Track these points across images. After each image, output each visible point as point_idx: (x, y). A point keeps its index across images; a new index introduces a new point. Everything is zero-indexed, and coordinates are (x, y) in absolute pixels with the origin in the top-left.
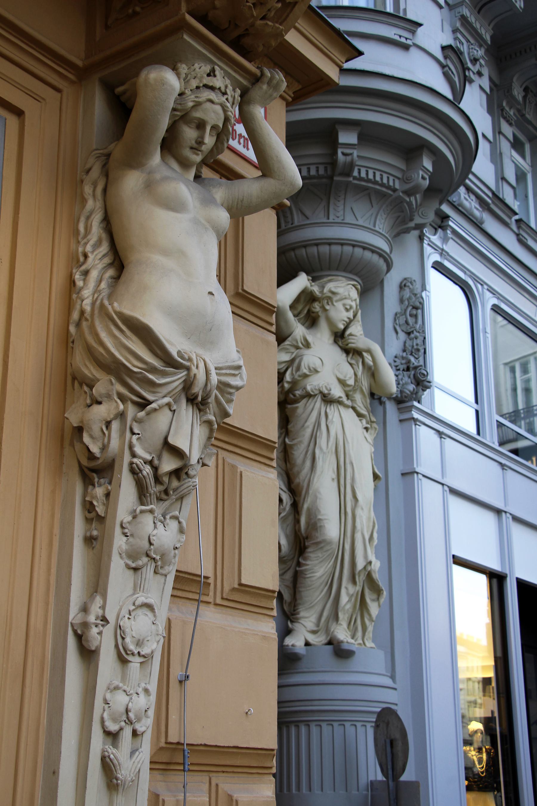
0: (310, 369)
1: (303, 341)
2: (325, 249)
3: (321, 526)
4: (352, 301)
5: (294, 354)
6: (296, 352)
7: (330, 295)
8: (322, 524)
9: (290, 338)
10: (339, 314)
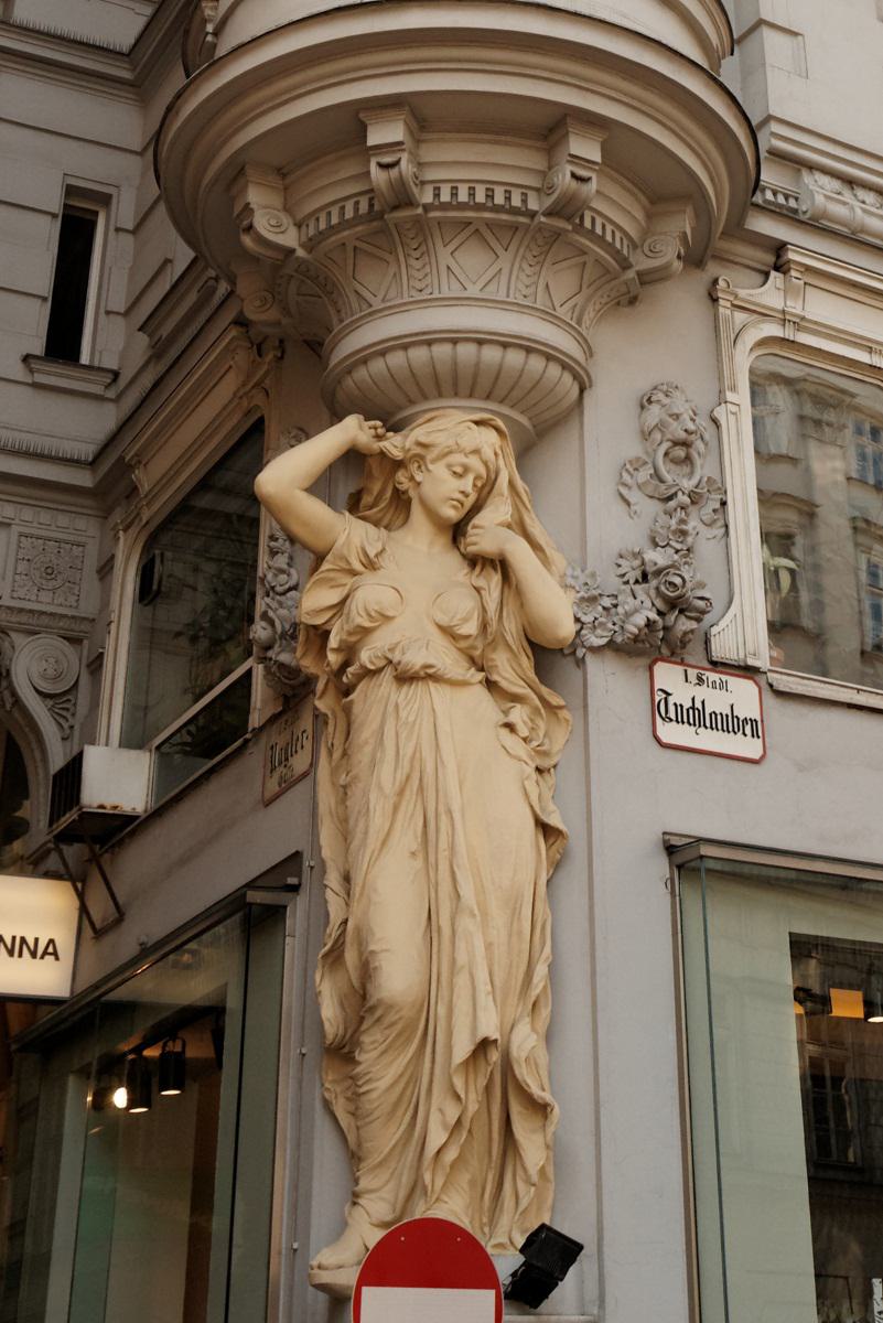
0: (369, 615)
1: (363, 560)
2: (396, 359)
3: (375, 968)
4: (466, 455)
5: (348, 587)
6: (349, 581)
7: (418, 450)
8: (377, 964)
9: (329, 557)
10: (442, 487)
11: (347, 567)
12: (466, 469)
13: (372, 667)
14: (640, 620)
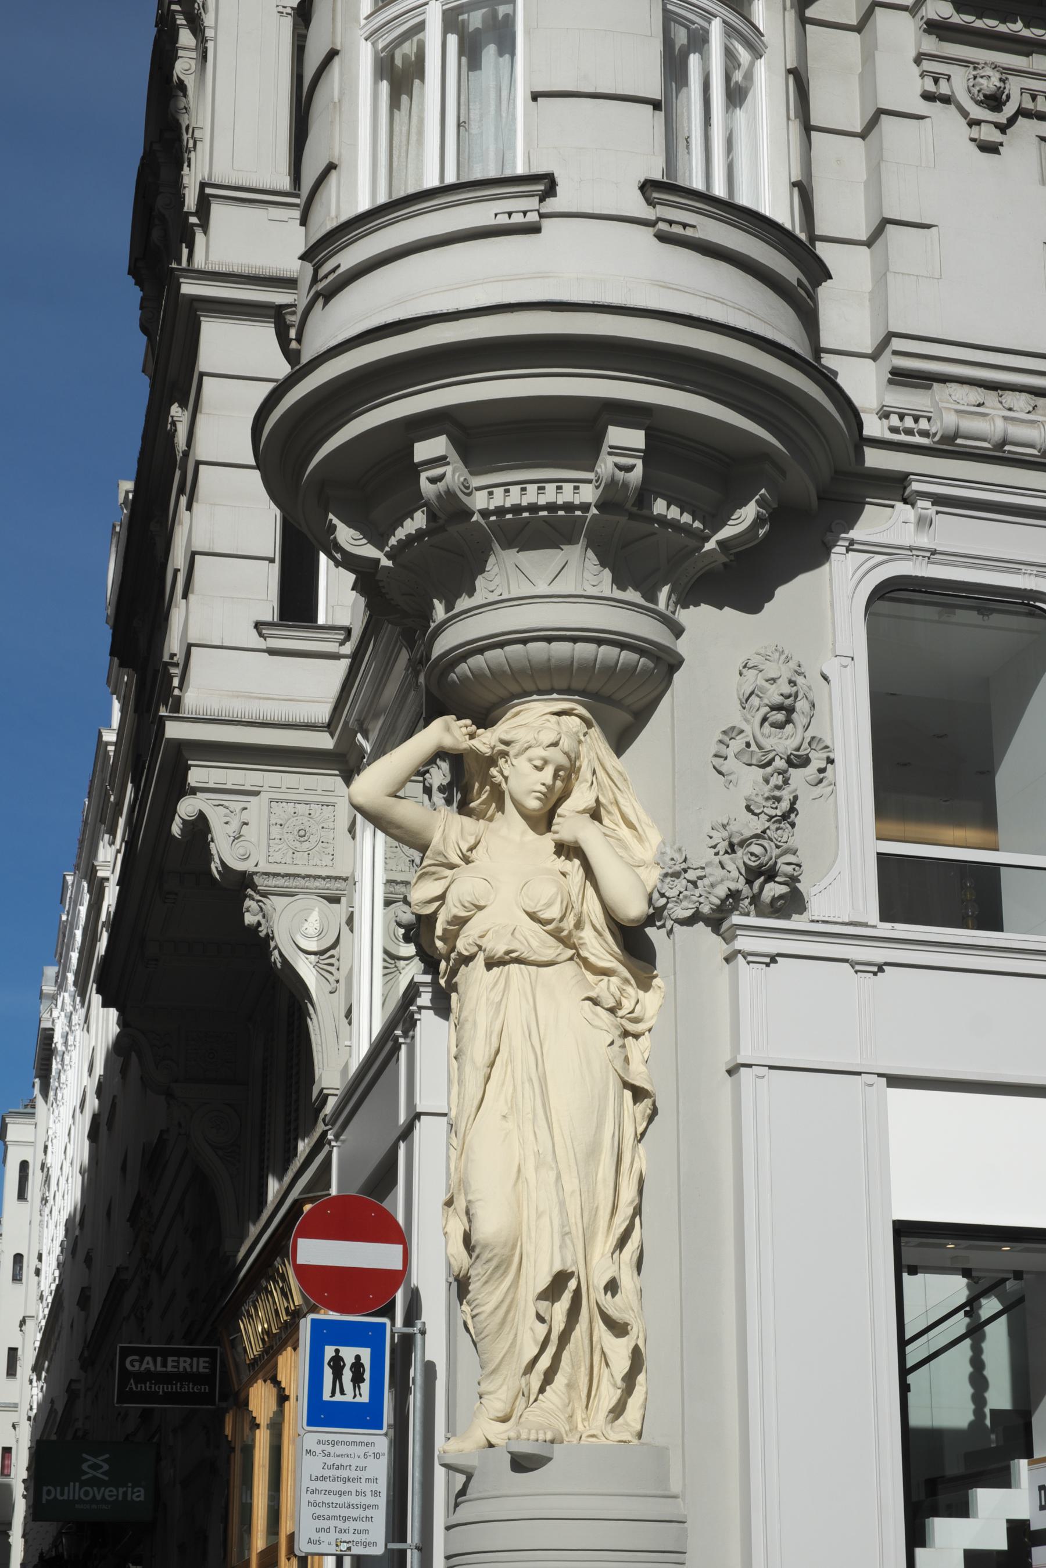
7: (503, 747)
9: (428, 853)
10: (524, 780)
11: (445, 861)
12: (546, 762)
13: (466, 953)
14: (722, 891)
